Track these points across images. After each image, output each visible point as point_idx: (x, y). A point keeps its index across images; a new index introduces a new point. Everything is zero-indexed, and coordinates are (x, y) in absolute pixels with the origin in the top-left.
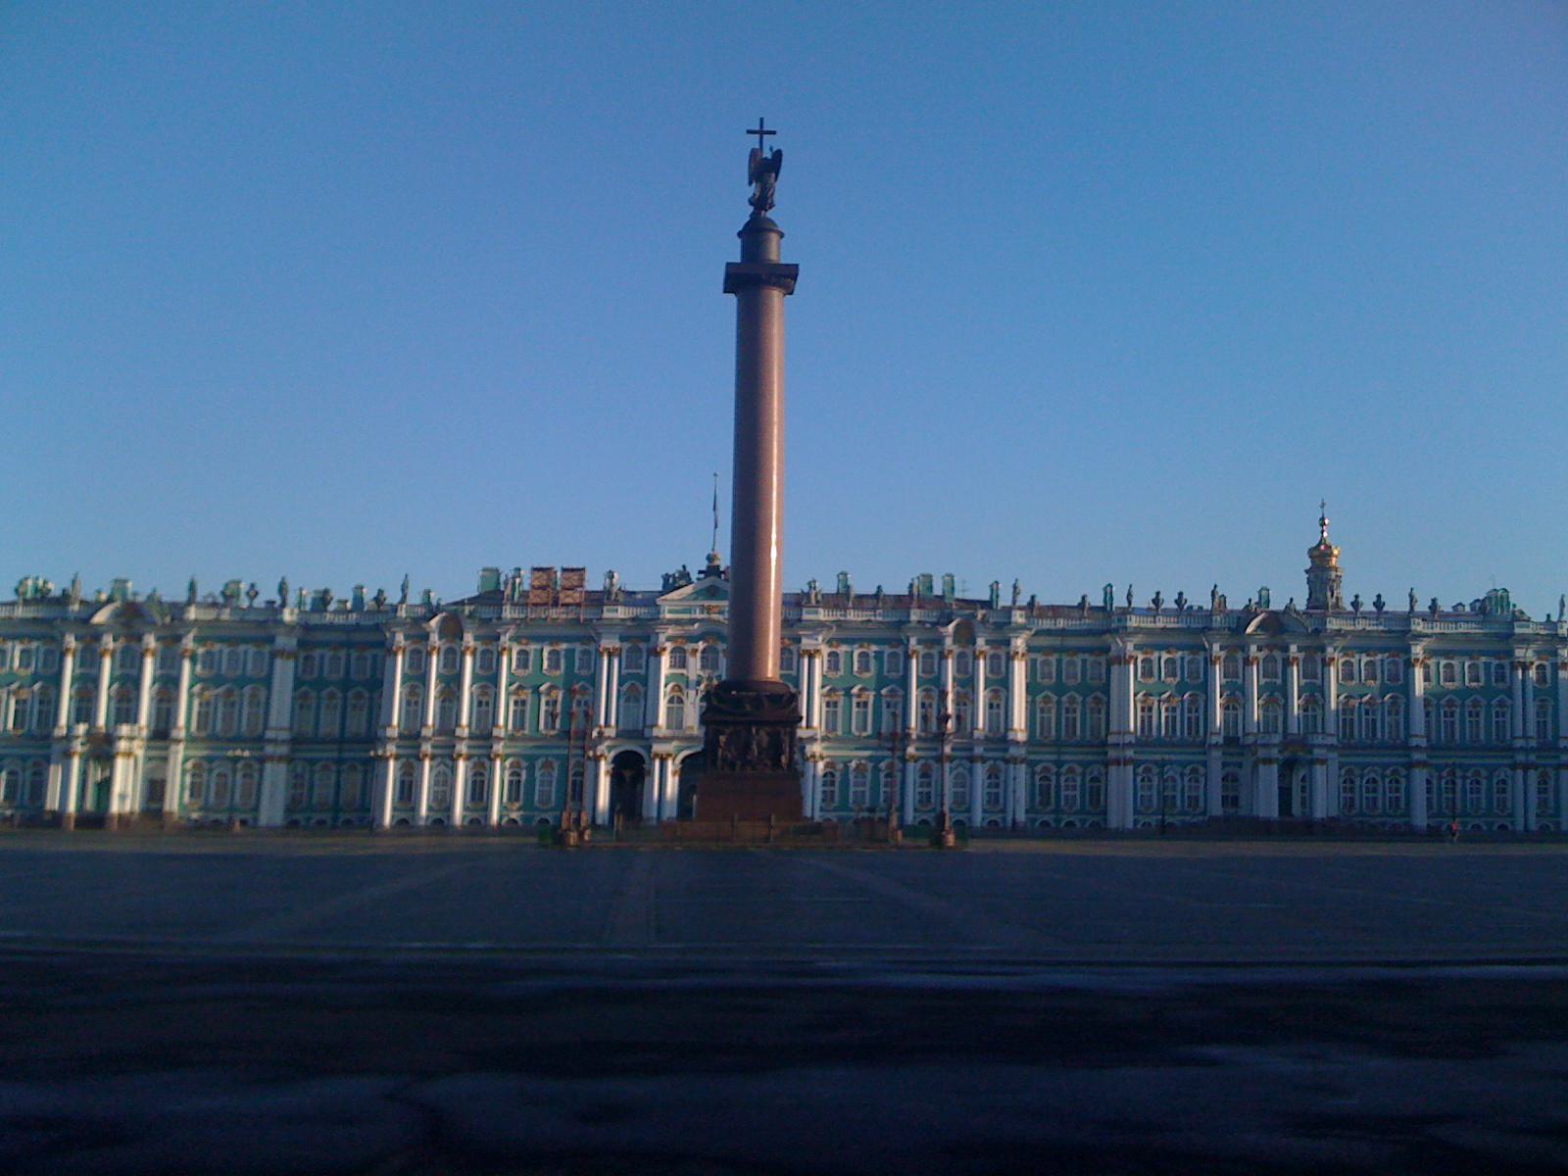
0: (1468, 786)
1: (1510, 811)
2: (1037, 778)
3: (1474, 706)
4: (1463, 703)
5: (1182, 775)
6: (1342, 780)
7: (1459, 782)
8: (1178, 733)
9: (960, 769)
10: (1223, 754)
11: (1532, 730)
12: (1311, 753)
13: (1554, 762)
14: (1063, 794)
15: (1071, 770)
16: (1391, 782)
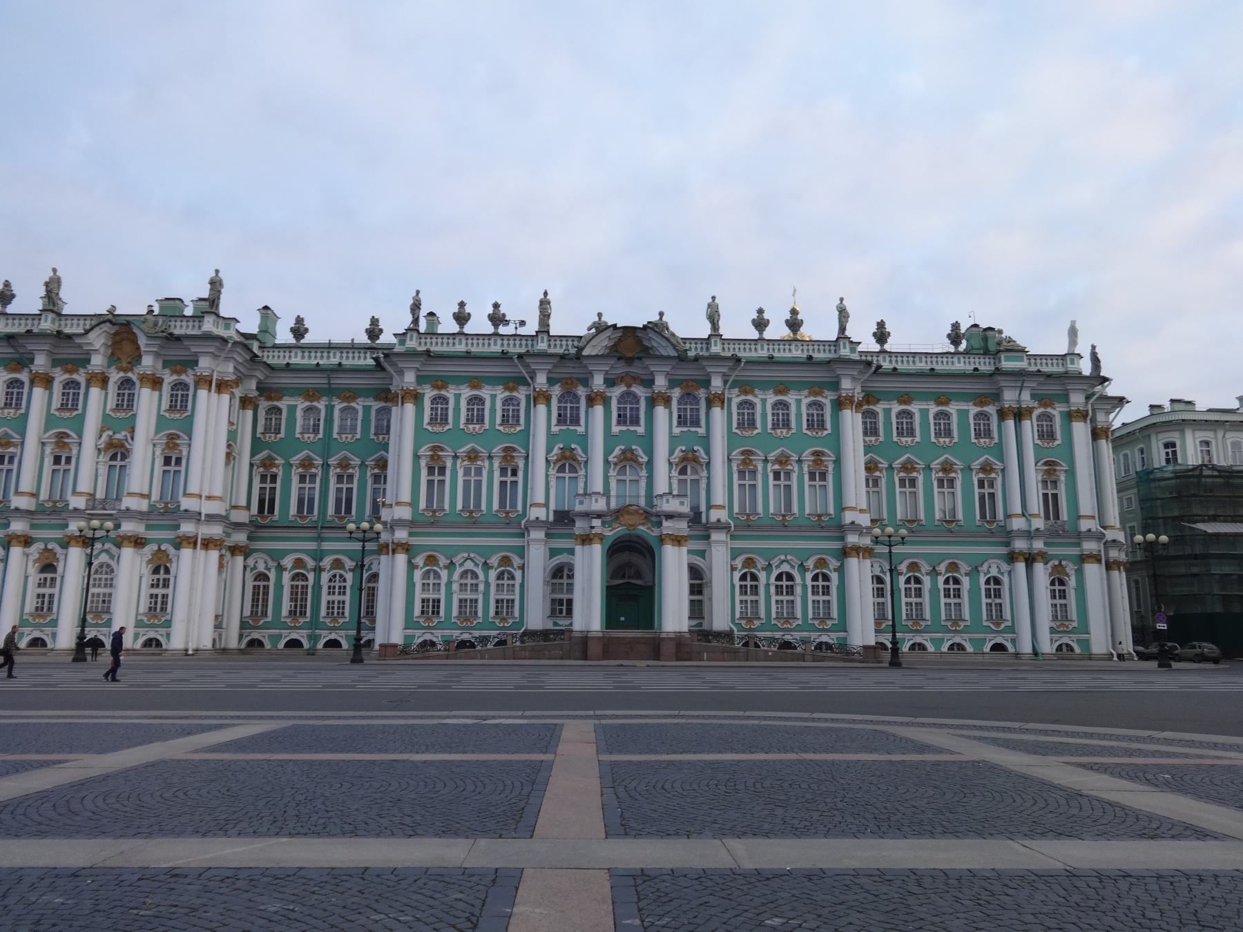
0: (941, 586)
1: (1009, 624)
2: (286, 576)
3: (944, 470)
4: (928, 468)
5: (487, 567)
6: (737, 575)
7: (927, 580)
8: (484, 507)
9: (104, 558)
10: (547, 535)
11: (1035, 505)
12: (660, 524)
13: (1075, 551)
14: (325, 598)
15: (337, 564)
16: (815, 578)
